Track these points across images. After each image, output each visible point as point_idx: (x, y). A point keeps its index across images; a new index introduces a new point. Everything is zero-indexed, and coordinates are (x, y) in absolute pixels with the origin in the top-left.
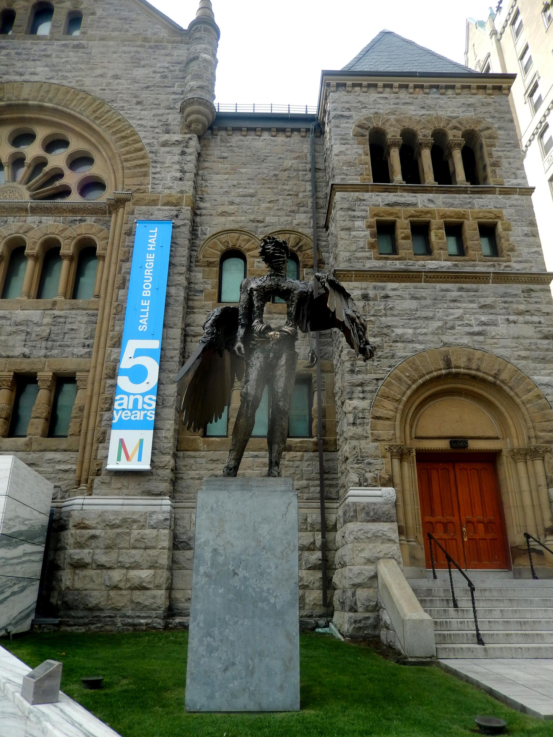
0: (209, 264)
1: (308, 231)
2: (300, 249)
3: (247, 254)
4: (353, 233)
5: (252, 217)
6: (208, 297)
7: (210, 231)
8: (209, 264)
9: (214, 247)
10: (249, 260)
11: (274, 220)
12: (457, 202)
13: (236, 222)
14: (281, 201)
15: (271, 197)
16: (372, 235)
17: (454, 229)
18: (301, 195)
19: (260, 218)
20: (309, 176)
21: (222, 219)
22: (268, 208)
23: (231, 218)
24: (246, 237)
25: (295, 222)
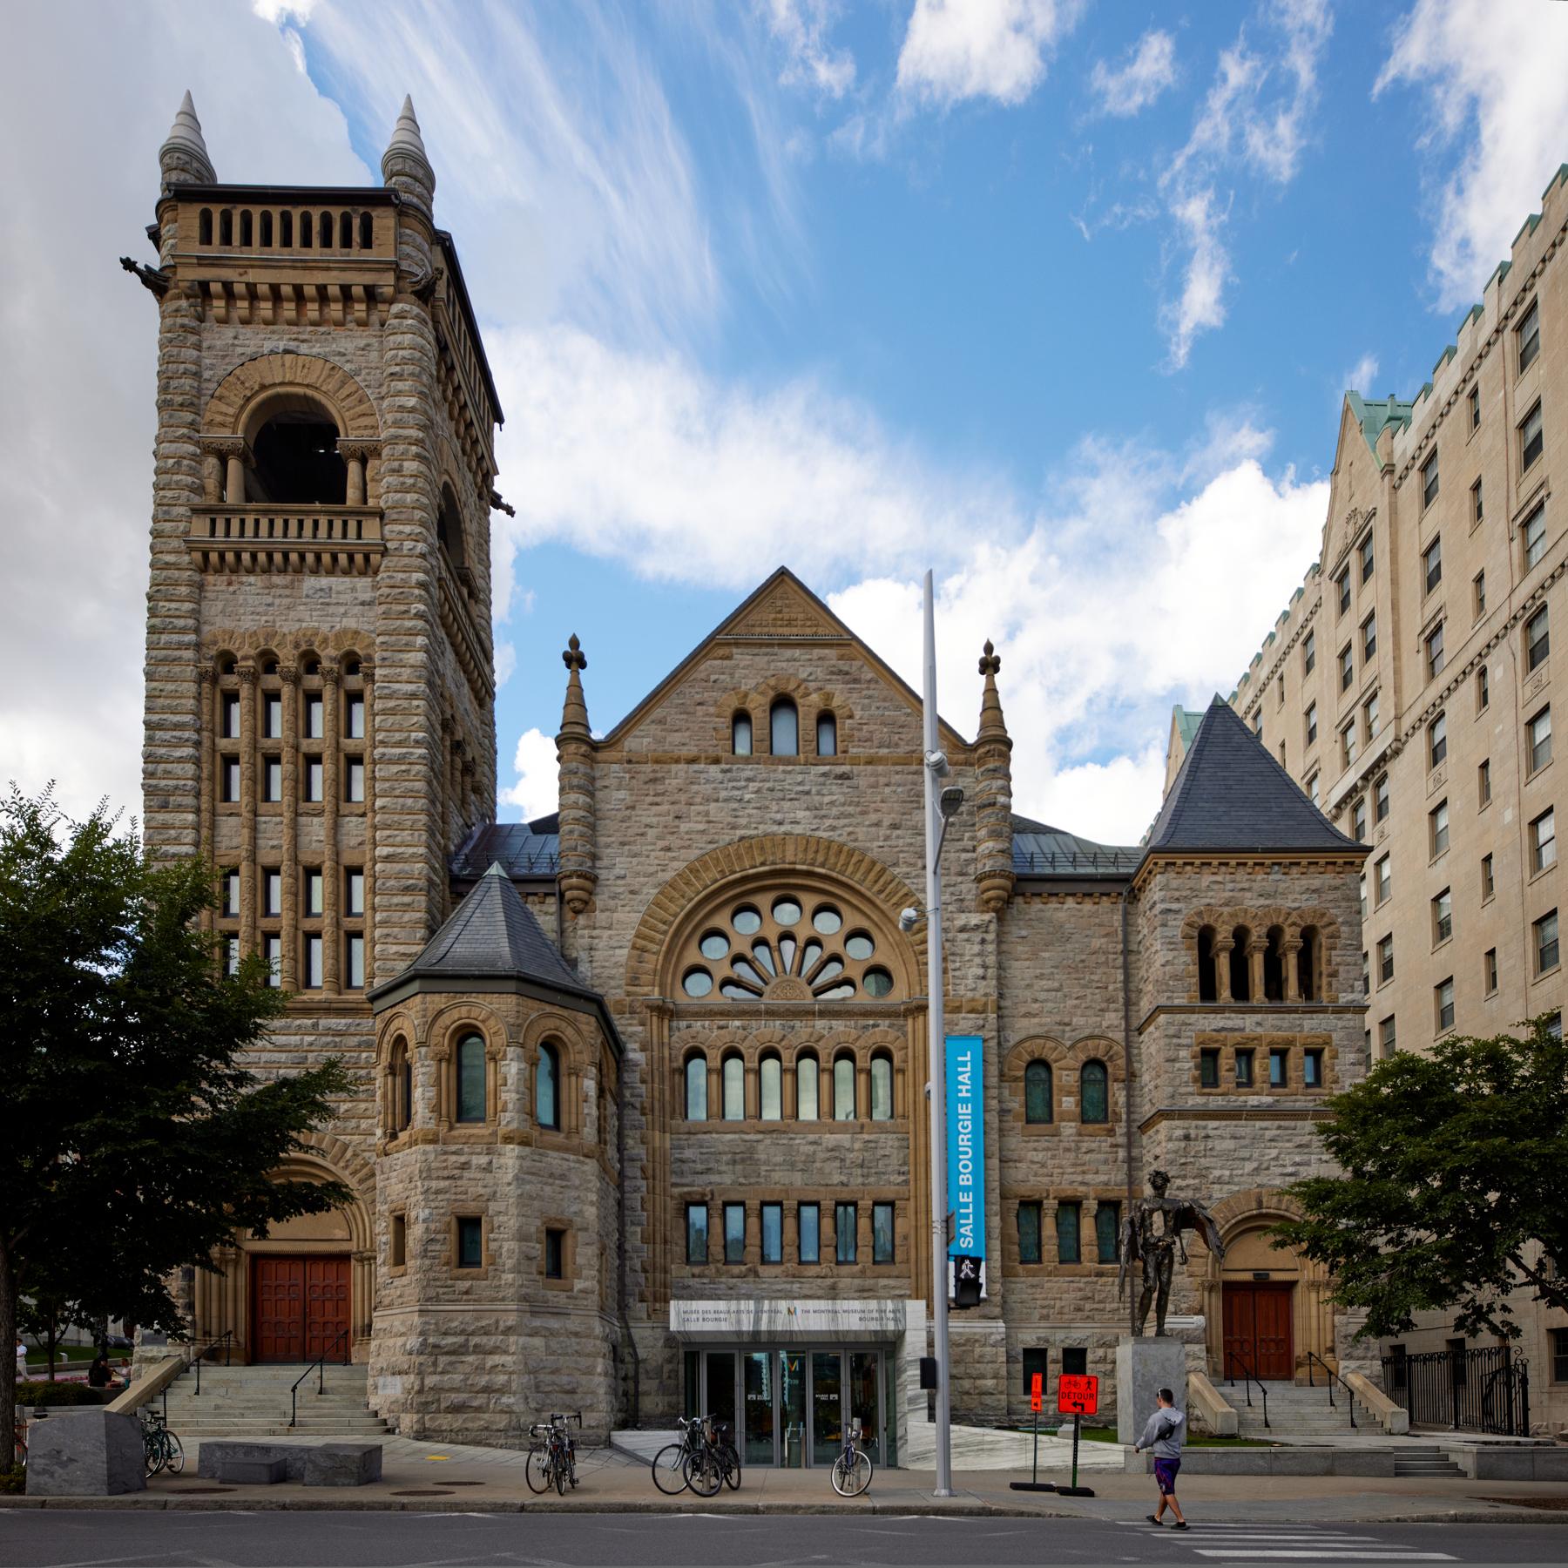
0: (1016, 1079)
1: (1119, 1036)
2: (1111, 1059)
3: (1054, 1066)
4: (1177, 1065)
5: (1058, 1019)
6: (1016, 1118)
7: (1013, 1038)
8: (1016, 1079)
9: (1019, 1057)
10: (1055, 1071)
11: (1082, 1021)
12: (1286, 1024)
13: (1041, 1025)
14: (1089, 997)
15: (1077, 991)
16: (1197, 1067)
17: (1281, 1053)
18: (1111, 987)
19: (1067, 1020)
20: (1121, 960)
21: (1025, 1022)
22: (1076, 1007)
23: (1036, 1020)
24: (1051, 1044)
25: (1105, 1024)
